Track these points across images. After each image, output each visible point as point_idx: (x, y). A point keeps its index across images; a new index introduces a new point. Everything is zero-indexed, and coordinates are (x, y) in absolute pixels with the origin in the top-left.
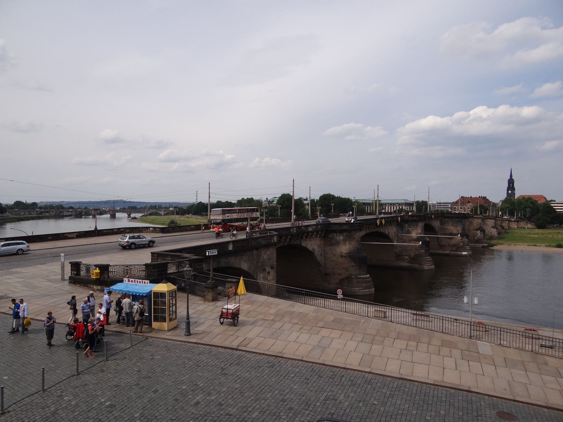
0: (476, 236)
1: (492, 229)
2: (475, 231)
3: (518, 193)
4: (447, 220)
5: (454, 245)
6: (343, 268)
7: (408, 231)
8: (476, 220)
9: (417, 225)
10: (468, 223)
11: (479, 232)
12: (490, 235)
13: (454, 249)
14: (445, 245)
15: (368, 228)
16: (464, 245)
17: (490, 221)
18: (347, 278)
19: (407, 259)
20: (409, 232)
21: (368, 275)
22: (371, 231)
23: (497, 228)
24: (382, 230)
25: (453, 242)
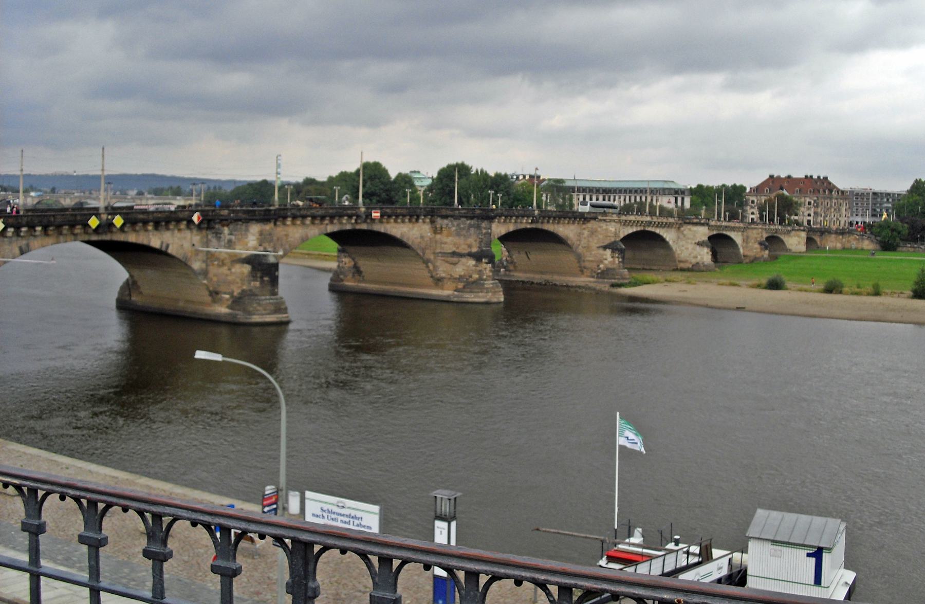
1: (698, 247)
2: (601, 251)
4: (446, 221)
5: (460, 279)
7: (230, 241)
9: (247, 230)
10: (586, 233)
11: (608, 252)
12: (694, 261)
13: (460, 286)
16: (481, 279)
17: (695, 228)
19: (227, 300)
20: (230, 244)
24: (132, 238)
25: (459, 270)
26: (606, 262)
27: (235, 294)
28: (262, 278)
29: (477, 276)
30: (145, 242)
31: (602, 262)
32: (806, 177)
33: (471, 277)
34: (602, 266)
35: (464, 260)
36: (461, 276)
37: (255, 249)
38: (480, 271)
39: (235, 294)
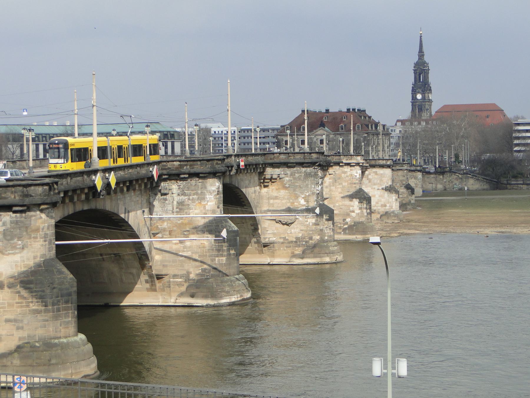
0: (348, 215)
2: (347, 202)
3: (439, 100)
5: (297, 242)
6: (7, 321)
8: (347, 169)
11: (356, 202)
13: (299, 251)
14: (273, 243)
15: (72, 200)
16: (322, 240)
18: (19, 348)
21: (82, 336)
22: (79, 207)
23: (397, 192)
24: (107, 205)
25: (295, 231)
26: (353, 214)
27: (192, 276)
28: (229, 250)
29: (318, 237)
30: (116, 212)
31: (348, 215)
32: (348, 110)
33: (311, 238)
34: (348, 220)
35: (300, 218)
36: (297, 238)
37: (214, 212)
38: (321, 230)
39: (192, 276)
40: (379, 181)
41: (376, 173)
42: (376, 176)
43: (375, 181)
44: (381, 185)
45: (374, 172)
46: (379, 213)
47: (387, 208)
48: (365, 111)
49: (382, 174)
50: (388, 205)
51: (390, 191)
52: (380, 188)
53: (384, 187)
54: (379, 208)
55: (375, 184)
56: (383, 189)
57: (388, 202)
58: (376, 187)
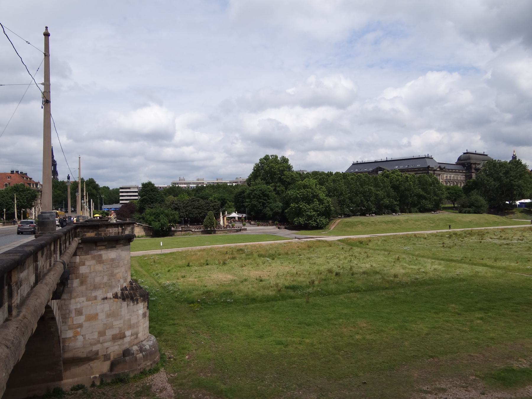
12: (115, 349)
17: (111, 254)
40: (105, 279)
41: (100, 260)
42: (99, 267)
43: (97, 280)
44: (111, 287)
45: (93, 258)
46: (106, 357)
47: (127, 339)
48: (26, 174)
49: (113, 260)
50: (128, 333)
51: (132, 299)
52: (110, 295)
53: (118, 290)
54: (106, 345)
55: (96, 288)
56: (116, 296)
57: (130, 327)
58: (100, 294)
